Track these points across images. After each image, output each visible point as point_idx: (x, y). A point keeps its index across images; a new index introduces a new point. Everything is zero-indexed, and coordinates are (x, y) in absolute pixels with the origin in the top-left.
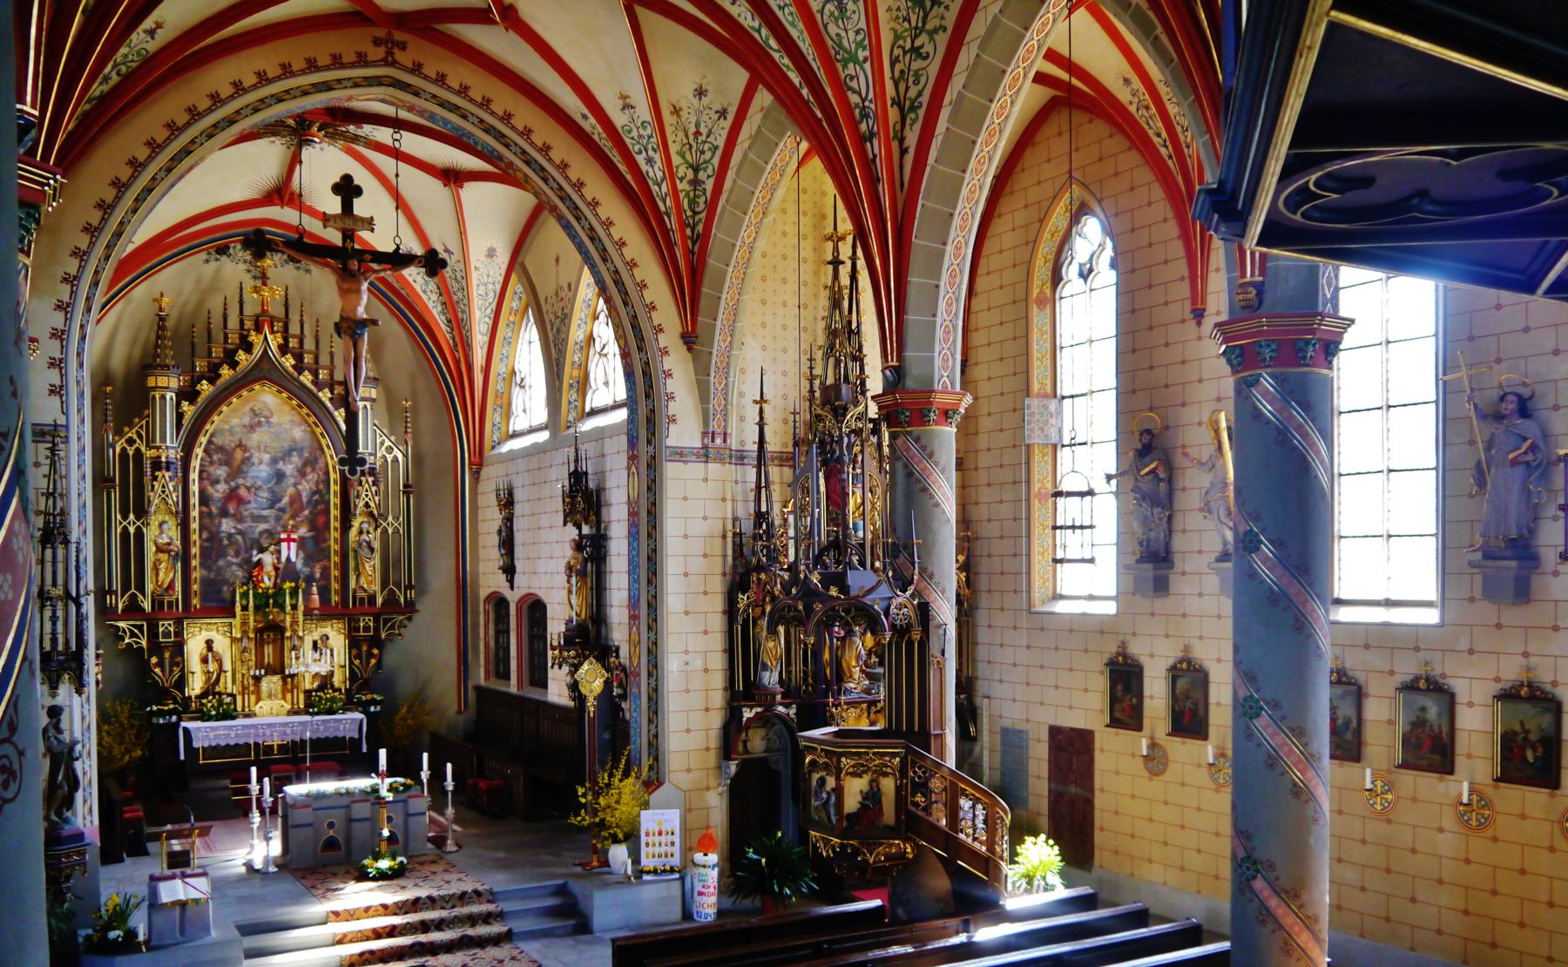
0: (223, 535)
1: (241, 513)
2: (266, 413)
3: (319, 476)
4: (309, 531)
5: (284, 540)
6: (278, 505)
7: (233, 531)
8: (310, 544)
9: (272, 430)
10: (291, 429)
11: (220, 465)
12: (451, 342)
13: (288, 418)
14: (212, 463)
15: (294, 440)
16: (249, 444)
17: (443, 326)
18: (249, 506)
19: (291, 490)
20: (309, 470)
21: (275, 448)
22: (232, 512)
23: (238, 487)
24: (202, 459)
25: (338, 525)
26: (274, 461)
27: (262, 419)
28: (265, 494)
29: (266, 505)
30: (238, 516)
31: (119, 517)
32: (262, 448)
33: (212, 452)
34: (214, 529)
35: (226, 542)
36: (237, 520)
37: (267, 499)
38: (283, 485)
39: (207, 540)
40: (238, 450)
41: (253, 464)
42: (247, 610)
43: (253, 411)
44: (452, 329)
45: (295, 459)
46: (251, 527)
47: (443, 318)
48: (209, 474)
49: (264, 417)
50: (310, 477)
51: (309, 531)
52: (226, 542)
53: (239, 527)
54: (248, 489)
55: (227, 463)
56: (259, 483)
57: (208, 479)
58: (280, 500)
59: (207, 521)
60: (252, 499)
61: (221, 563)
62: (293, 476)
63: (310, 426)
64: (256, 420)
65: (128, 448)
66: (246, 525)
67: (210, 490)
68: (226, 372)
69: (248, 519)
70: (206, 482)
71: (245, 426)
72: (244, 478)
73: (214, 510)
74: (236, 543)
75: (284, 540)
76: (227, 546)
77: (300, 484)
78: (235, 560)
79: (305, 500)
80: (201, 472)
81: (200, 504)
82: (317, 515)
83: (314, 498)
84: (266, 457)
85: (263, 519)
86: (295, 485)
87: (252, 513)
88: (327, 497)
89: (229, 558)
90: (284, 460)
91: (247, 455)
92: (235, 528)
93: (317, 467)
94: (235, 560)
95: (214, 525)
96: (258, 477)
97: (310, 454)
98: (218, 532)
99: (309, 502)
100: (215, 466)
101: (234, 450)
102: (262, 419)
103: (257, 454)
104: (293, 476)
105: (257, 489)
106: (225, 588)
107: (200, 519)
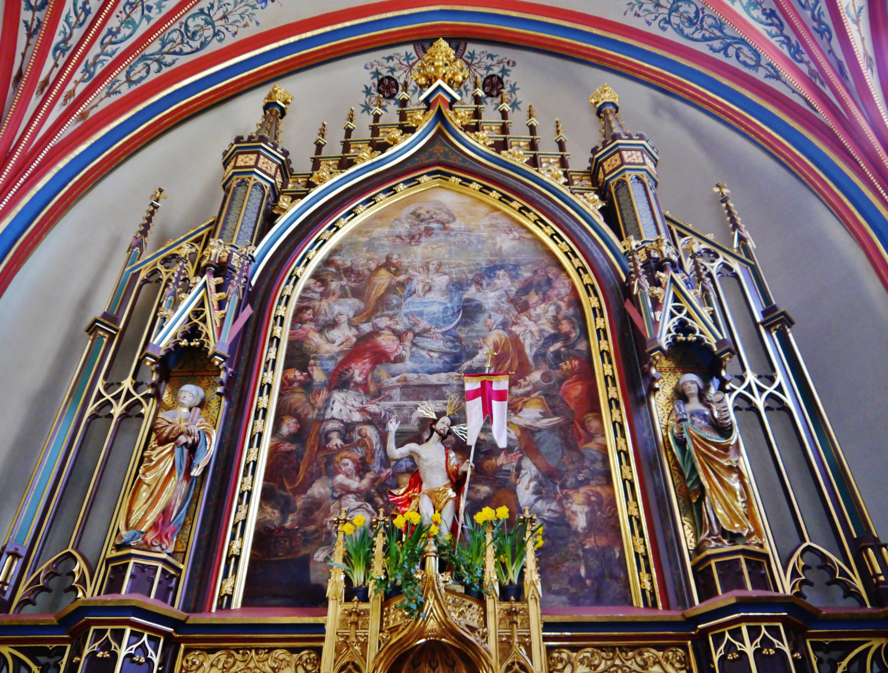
0: (331, 426)
1: (378, 381)
2: (444, 217)
3: (558, 309)
4: (545, 415)
5: (473, 395)
6: (466, 365)
7: (357, 417)
8: (550, 445)
9: (452, 239)
10: (493, 238)
11: (344, 295)
12: (785, 50)
13: (486, 221)
14: (324, 295)
15: (499, 253)
16: (405, 261)
17: (760, 28)
18: (398, 366)
19: (496, 336)
20: (533, 298)
21: (458, 265)
22: (359, 379)
23: (376, 332)
24: (306, 289)
25: (616, 392)
26: (458, 285)
27: (434, 225)
28: (436, 344)
29: (439, 364)
30: (372, 388)
31: (100, 385)
32: (431, 267)
33: (329, 278)
34: (313, 415)
35: (336, 441)
36: (367, 392)
37: (446, 353)
38: (479, 326)
39: (296, 437)
40: (383, 272)
41: (412, 293)
42: (365, 599)
43: (416, 215)
44: (781, 26)
45: (503, 281)
46: (399, 408)
47: (757, 13)
48: (315, 314)
49: (438, 222)
50: (539, 310)
51: (545, 415)
52: (336, 441)
53: (373, 408)
54: (400, 336)
55: (357, 293)
56: (424, 324)
57: (313, 320)
58: (471, 355)
59: (297, 398)
60: (406, 354)
61: (318, 489)
62: (499, 310)
63: (529, 231)
64: (422, 226)
65: (163, 270)
66: (388, 404)
67: (316, 339)
68: (366, 158)
69: (396, 393)
70: (308, 326)
71: (399, 237)
72: (391, 318)
73: (319, 376)
74: (363, 442)
75: (473, 395)
76: (340, 450)
77: (515, 324)
78: (354, 483)
79: (529, 352)
80: (299, 311)
81: (287, 367)
82: (561, 381)
83: (552, 349)
84: (441, 281)
85: (436, 392)
86: (504, 325)
87: (405, 380)
88: (582, 346)
89: (340, 478)
90: (479, 284)
91: (401, 278)
92: (362, 410)
93: (553, 293)
94: (354, 483)
95: (313, 407)
96: (421, 314)
97: (535, 272)
98: (321, 420)
99: (540, 356)
100: (332, 299)
101: (374, 272)
102: (434, 225)
103: (421, 277)
104: (499, 310)
105: (416, 335)
106: (320, 556)
107: (281, 395)
